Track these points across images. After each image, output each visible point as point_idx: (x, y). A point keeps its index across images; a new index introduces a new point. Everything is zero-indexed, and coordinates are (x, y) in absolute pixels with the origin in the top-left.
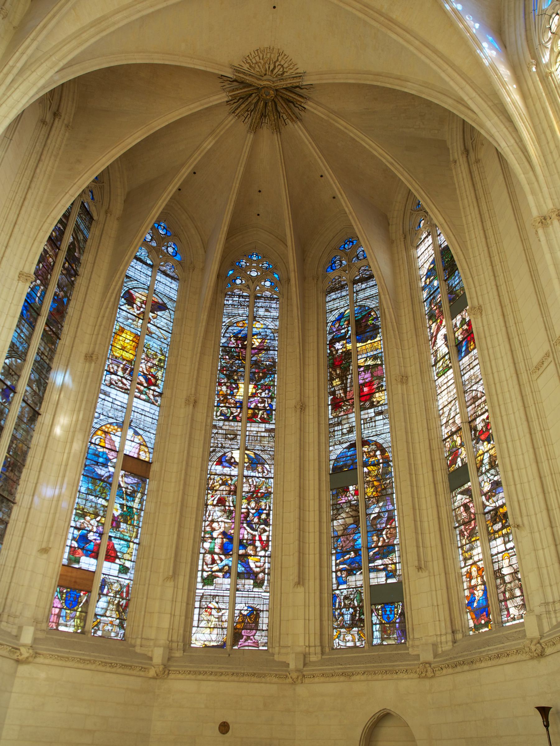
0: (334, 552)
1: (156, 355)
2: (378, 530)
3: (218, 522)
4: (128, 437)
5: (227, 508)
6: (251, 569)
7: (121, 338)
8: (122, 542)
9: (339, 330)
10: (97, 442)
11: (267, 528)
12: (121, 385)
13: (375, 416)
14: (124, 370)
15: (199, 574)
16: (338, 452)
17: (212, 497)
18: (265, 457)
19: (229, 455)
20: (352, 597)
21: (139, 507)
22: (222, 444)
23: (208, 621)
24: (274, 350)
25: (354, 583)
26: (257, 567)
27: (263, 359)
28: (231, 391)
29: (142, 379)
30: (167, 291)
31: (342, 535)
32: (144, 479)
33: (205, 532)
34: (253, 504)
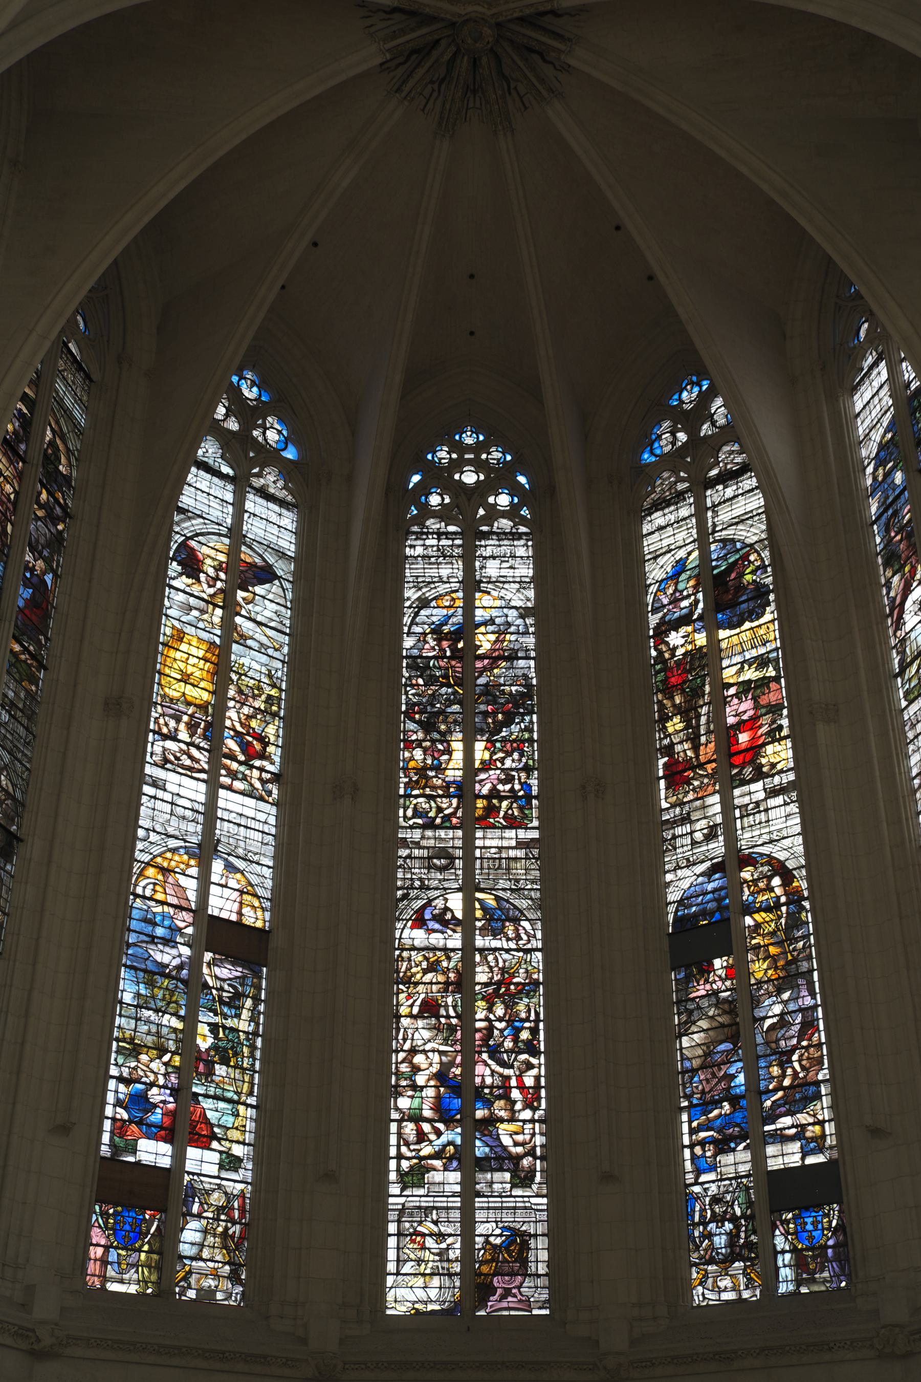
0: (686, 1104)
1: (260, 688)
2: (783, 1053)
3: (425, 1052)
4: (215, 878)
5: (443, 1020)
7: (178, 655)
8: (222, 1105)
9: (675, 601)
10: (148, 893)
11: (534, 1061)
12: (188, 762)
13: (766, 799)
14: (192, 727)
15: (393, 1164)
16: (685, 884)
17: (409, 997)
18: (523, 904)
19: (440, 903)
20: (728, 1197)
21: (251, 1029)
22: (420, 879)
23: (419, 1261)
24: (527, 658)
25: (731, 1169)
26: (516, 1144)
27: (502, 680)
28: (434, 758)
29: (232, 744)
30: (272, 535)
31: (702, 1067)
32: (256, 969)
33: (398, 1074)
34: (500, 1011)
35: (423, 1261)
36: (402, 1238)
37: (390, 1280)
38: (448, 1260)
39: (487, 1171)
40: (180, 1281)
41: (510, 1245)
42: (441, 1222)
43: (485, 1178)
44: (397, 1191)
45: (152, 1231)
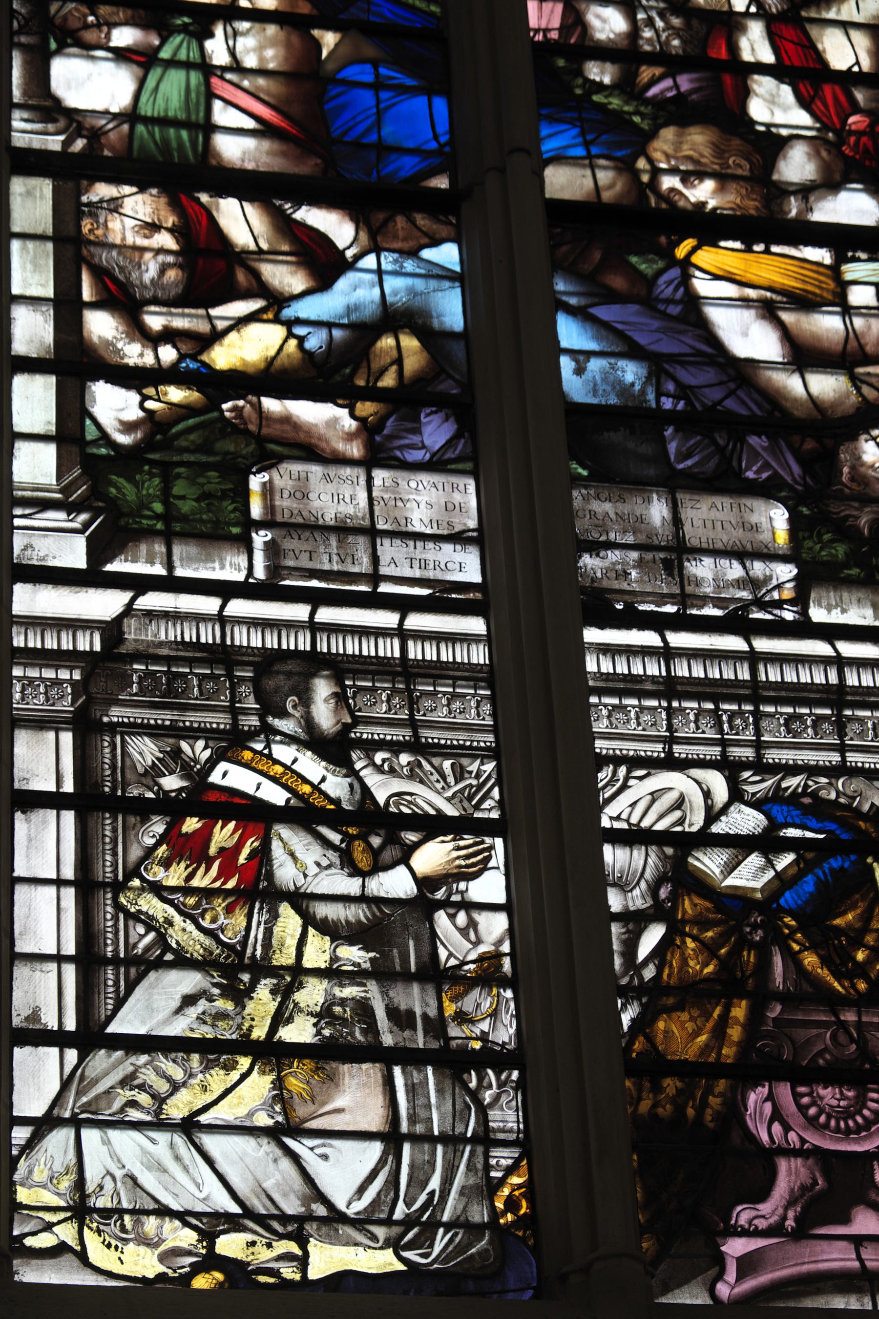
6: (744, 372)
26: (803, 355)
35: (262, 968)
36: (107, 826)
37: (37, 1078)
38: (434, 974)
39: (642, 485)
41: (831, 898)
42: (370, 747)
43: (639, 522)
44: (73, 554)
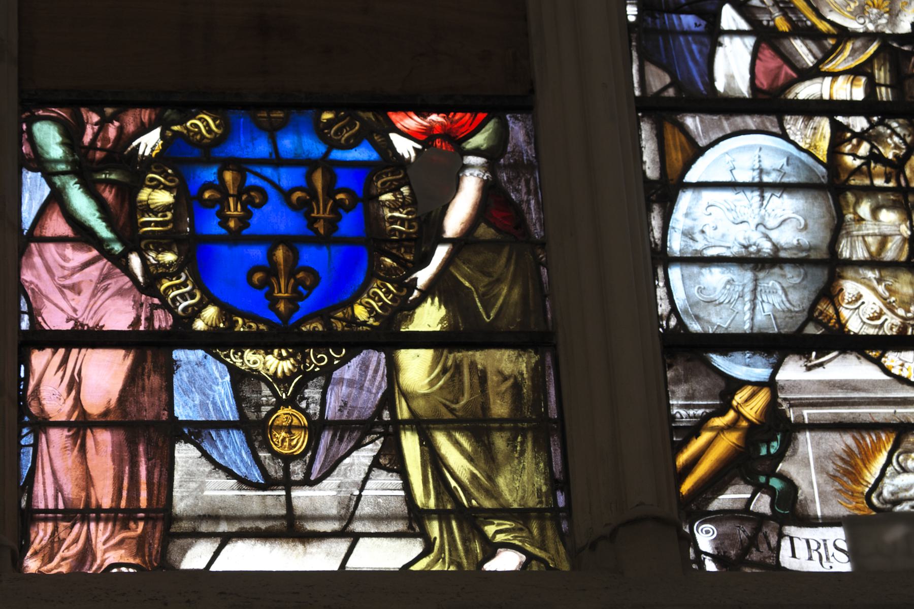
40: (717, 481)
45: (456, 218)
